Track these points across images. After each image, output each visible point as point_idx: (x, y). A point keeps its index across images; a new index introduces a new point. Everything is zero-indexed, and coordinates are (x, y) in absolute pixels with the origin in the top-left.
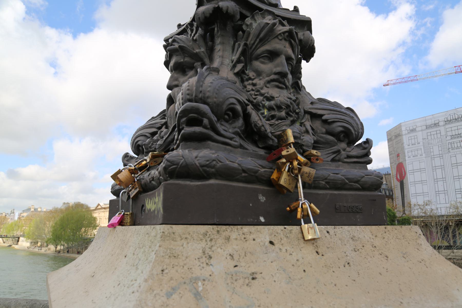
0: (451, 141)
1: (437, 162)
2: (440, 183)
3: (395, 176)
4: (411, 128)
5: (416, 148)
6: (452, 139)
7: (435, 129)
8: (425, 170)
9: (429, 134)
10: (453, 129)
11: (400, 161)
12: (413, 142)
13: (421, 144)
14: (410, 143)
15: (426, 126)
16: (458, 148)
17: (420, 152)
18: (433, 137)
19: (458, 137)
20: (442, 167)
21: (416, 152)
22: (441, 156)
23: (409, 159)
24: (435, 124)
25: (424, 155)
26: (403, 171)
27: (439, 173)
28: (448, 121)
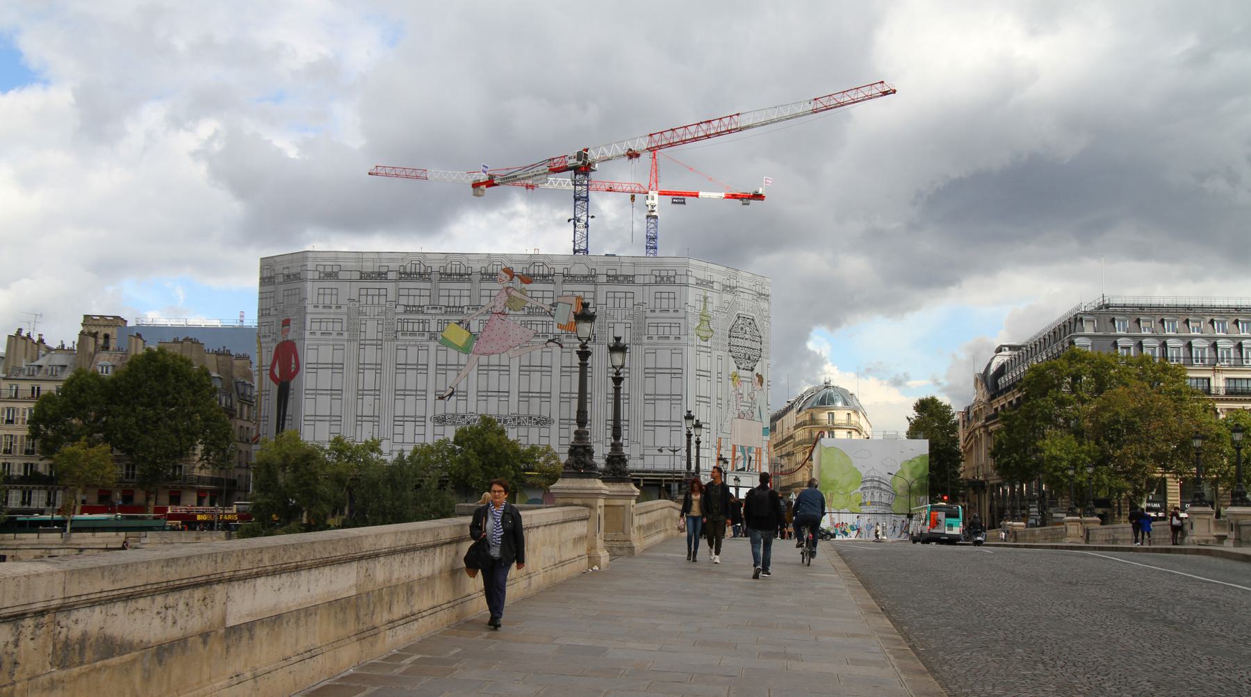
0: (403, 317)
1: (370, 355)
2: (368, 399)
3: (269, 368)
4: (328, 269)
5: (332, 316)
6: (405, 312)
7: (378, 285)
8: (343, 369)
9: (363, 292)
10: (412, 292)
11: (290, 338)
12: (327, 302)
13: (344, 309)
14: (321, 301)
15: (361, 273)
16: (413, 333)
17: (338, 326)
19: (417, 312)
20: (378, 367)
22: (378, 344)
24: (380, 274)
25: (346, 335)
26: (293, 361)
27: (369, 378)
28: (405, 273)
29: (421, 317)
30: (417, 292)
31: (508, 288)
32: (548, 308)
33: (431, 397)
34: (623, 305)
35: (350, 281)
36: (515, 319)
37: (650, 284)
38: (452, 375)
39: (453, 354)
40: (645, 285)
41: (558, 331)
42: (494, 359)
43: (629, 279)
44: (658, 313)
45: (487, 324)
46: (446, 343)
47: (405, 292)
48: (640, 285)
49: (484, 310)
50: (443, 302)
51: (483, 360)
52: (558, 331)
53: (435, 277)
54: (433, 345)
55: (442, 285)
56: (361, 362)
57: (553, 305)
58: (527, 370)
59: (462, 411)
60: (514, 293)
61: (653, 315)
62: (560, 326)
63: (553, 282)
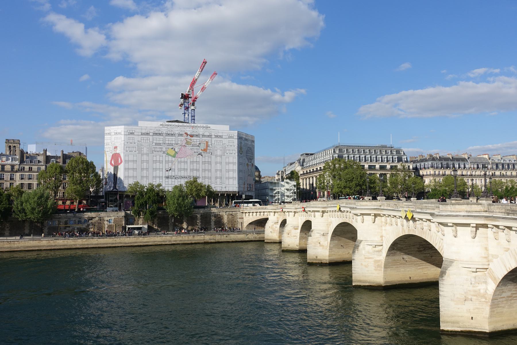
0: (155, 146)
1: (145, 158)
2: (145, 171)
4: (131, 132)
5: (133, 146)
6: (155, 145)
7: (147, 137)
10: (157, 139)
11: (118, 152)
12: (131, 142)
13: (136, 144)
14: (129, 141)
15: (142, 133)
16: (158, 151)
17: (134, 149)
18: (146, 142)
19: (159, 145)
20: (147, 162)
21: (132, 149)
22: (147, 154)
23: (127, 152)
24: (147, 133)
25: (137, 152)
26: (119, 159)
27: (145, 165)
28: (155, 133)
29: (160, 147)
30: (159, 139)
31: (186, 138)
32: (198, 145)
33: (164, 170)
34: (219, 144)
35: (138, 135)
36: (189, 147)
37: (227, 138)
38: (170, 164)
39: (170, 158)
40: (225, 138)
41: (201, 151)
42: (183, 159)
43: (221, 137)
44: (229, 147)
45: (180, 149)
46: (168, 154)
47: (155, 139)
48: (224, 138)
49: (179, 145)
50: (167, 142)
51: (179, 160)
53: (164, 135)
54: (164, 155)
55: (167, 137)
56: (142, 160)
57: (199, 144)
58: (192, 162)
59: (173, 175)
60: (188, 140)
61: (228, 147)
62: (202, 150)
63: (199, 137)
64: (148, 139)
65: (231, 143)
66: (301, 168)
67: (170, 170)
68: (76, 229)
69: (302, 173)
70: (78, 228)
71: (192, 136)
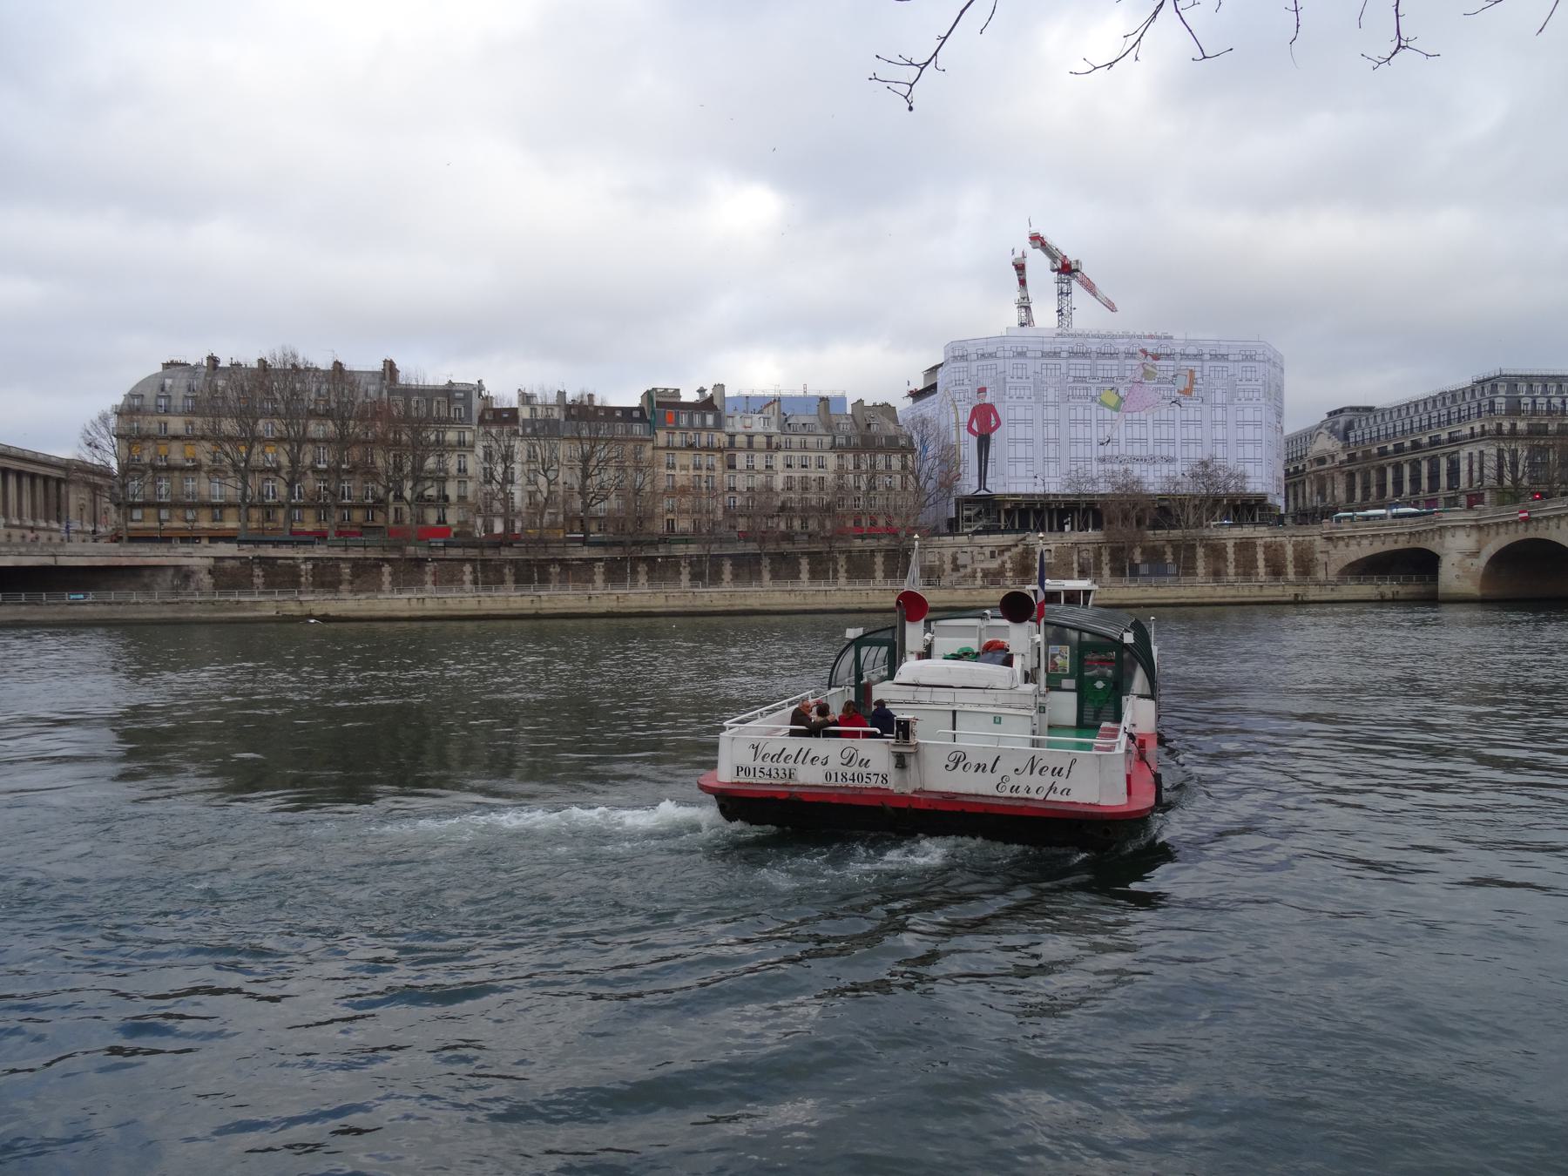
1: (1051, 413)
4: (1019, 350)
6: (1074, 381)
9: (1044, 366)
10: (1078, 367)
11: (987, 401)
13: (1031, 379)
15: (1043, 352)
17: (1027, 392)
19: (1082, 382)
20: (1057, 422)
22: (1056, 405)
24: (1055, 353)
25: (1033, 398)
26: (993, 418)
30: (1081, 367)
32: (1170, 378)
35: (1035, 358)
36: (1151, 385)
38: (1108, 427)
39: (1108, 411)
40: (1235, 361)
41: (1178, 395)
42: (1136, 416)
43: (1224, 357)
44: (1244, 382)
45: (1130, 390)
46: (1103, 404)
47: (1073, 367)
48: (1231, 361)
49: (1127, 380)
50: (1100, 374)
51: (1129, 416)
52: (1178, 395)
53: (1094, 356)
54: (1094, 405)
55: (1099, 362)
57: (1174, 376)
58: (1158, 423)
59: (1116, 453)
60: (1148, 368)
62: (1179, 391)
64: (1058, 367)
65: (1249, 373)
66: (1340, 444)
67: (1108, 442)
68: (979, 570)
69: (1344, 457)
70: (982, 569)
71: (1156, 357)
